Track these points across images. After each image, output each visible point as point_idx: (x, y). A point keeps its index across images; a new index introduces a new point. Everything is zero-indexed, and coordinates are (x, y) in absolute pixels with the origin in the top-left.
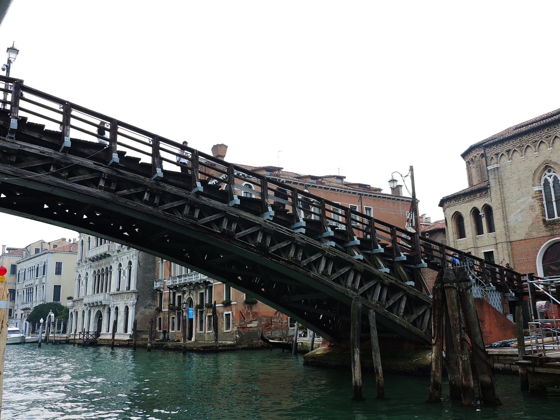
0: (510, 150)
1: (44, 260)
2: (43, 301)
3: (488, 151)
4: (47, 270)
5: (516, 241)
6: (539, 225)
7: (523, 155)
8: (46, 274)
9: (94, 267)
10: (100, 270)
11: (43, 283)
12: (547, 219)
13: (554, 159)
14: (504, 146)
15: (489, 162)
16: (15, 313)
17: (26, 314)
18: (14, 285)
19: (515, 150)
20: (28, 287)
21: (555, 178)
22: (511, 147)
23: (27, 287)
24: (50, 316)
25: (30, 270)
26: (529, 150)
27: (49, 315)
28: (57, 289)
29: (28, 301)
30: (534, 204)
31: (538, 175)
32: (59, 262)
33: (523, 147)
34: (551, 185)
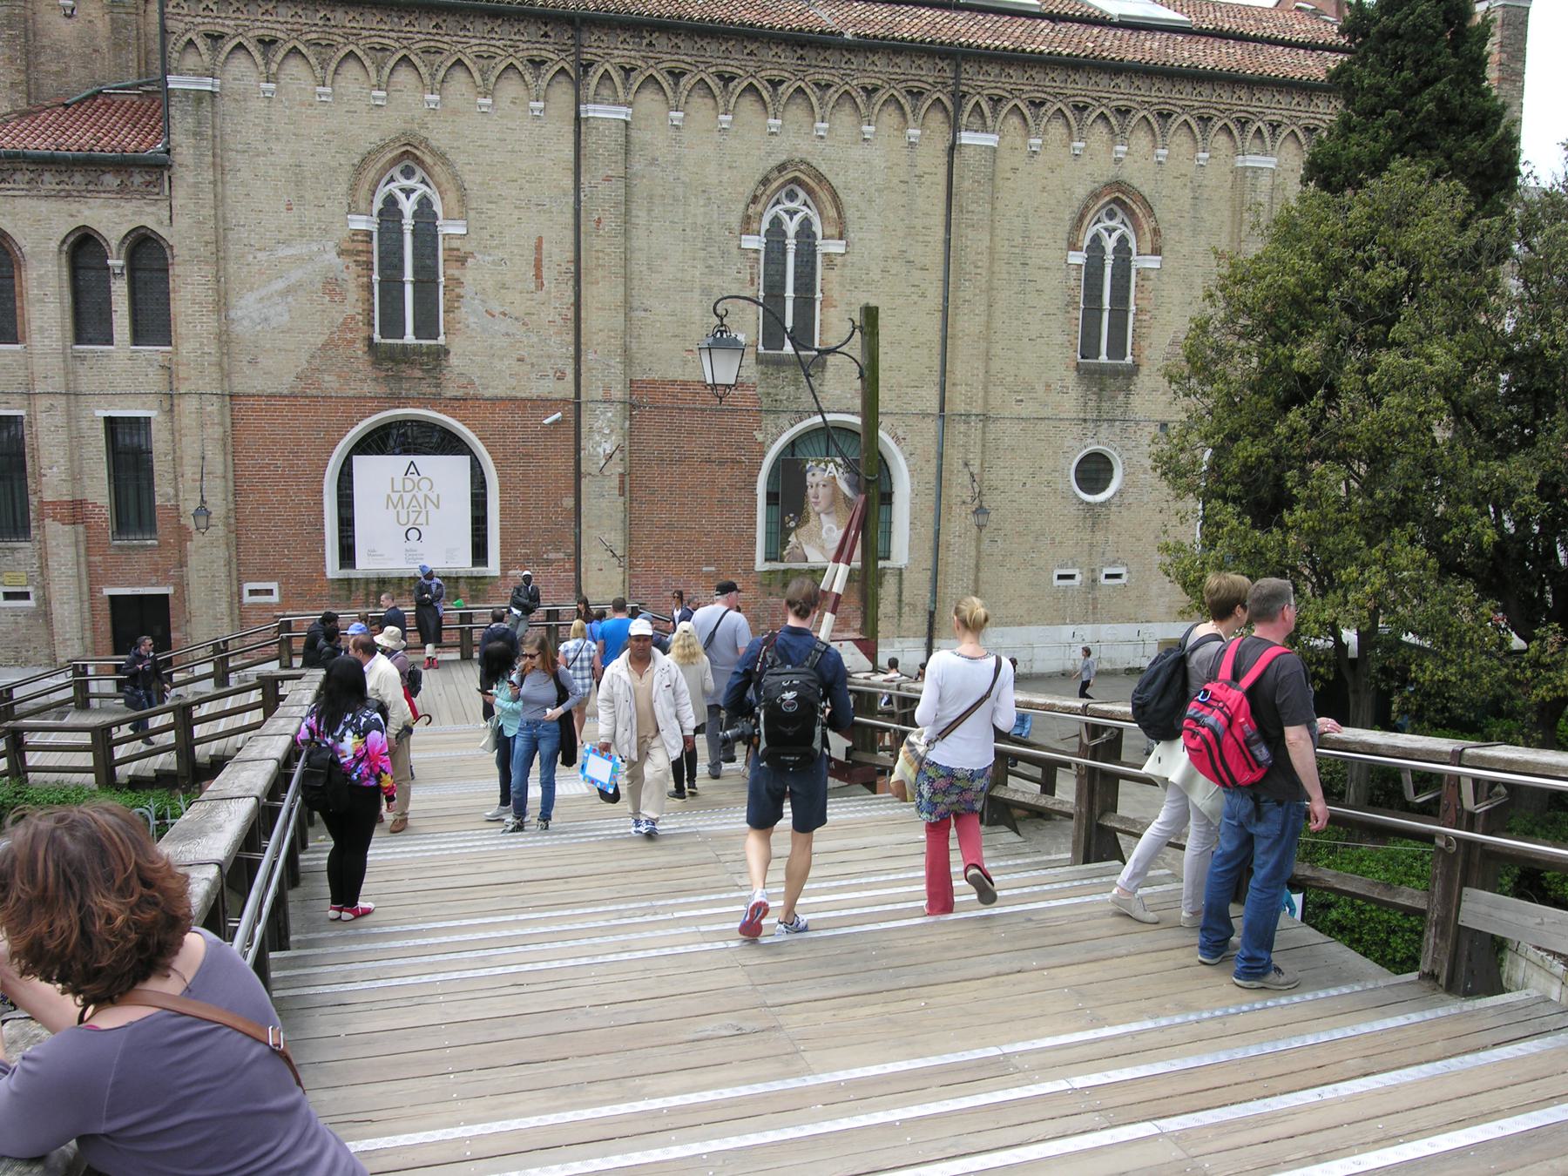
0: (274, 41)
3: (175, 11)
5: (254, 396)
6: (349, 352)
7: (328, 82)
12: (377, 337)
13: (439, 136)
14: (252, 18)
15: (175, 55)
19: (295, 51)
21: (425, 203)
22: (282, 31)
26: (351, 69)
30: (345, 276)
31: (371, 174)
33: (330, 52)
34: (408, 224)
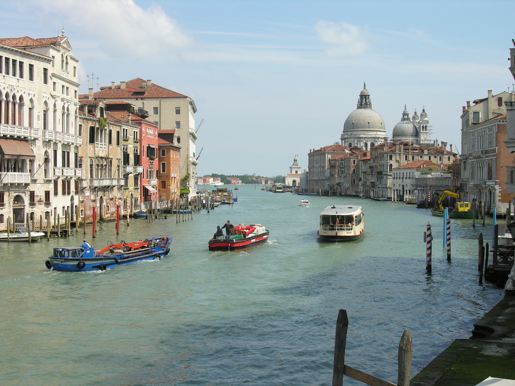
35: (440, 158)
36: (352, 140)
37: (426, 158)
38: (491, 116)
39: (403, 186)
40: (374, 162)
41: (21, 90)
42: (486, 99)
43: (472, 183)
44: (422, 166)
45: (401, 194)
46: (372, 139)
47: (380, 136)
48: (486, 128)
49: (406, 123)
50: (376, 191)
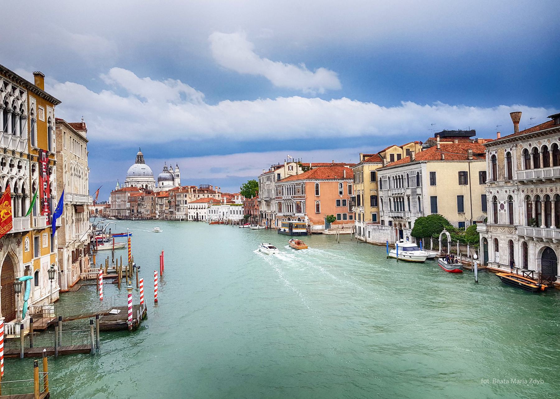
1: (417, 170)
2: (421, 213)
4: (422, 181)
8: (422, 185)
9: (526, 190)
10: (542, 196)
11: (417, 194)
16: (381, 219)
17: (397, 223)
18: (376, 192)
20: (396, 196)
23: (394, 196)
24: (444, 234)
25: (397, 179)
27: (442, 233)
28: (434, 200)
29: (398, 210)
32: (433, 172)
35: (214, 195)
36: (133, 183)
37: (206, 196)
38: (287, 176)
39: (197, 213)
40: (172, 199)
41: (80, 166)
42: (283, 166)
43: (282, 214)
44: (210, 201)
45: (196, 218)
46: (147, 183)
47: (151, 181)
48: (293, 184)
49: (166, 173)
50: (174, 217)
